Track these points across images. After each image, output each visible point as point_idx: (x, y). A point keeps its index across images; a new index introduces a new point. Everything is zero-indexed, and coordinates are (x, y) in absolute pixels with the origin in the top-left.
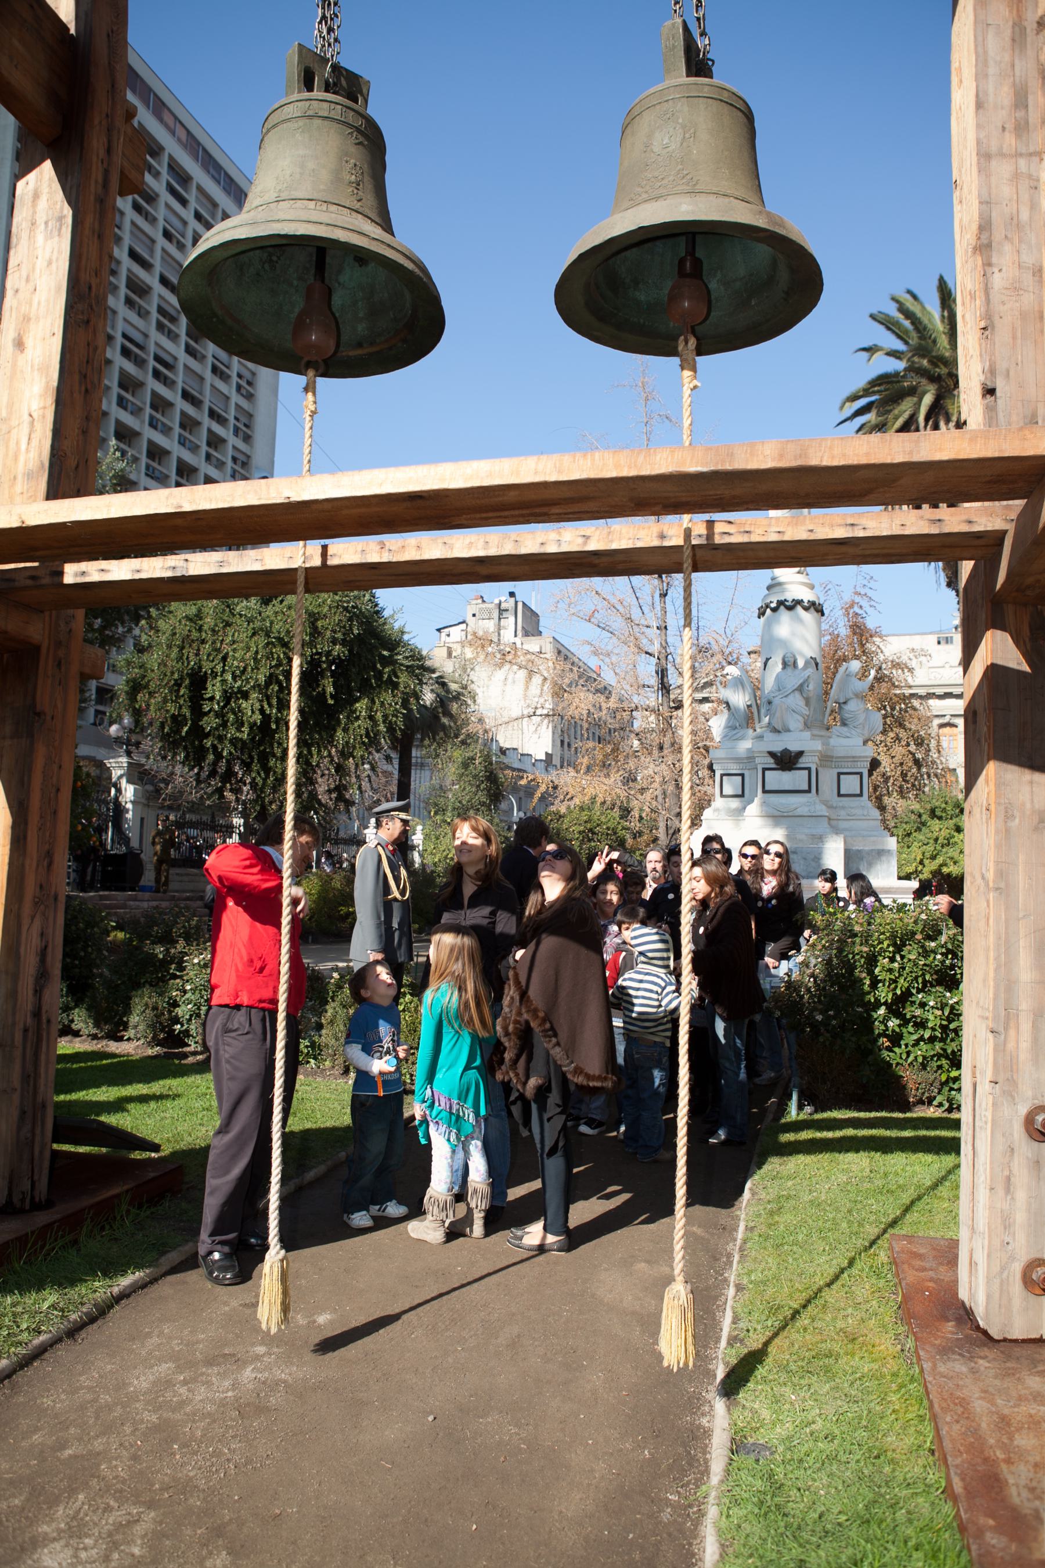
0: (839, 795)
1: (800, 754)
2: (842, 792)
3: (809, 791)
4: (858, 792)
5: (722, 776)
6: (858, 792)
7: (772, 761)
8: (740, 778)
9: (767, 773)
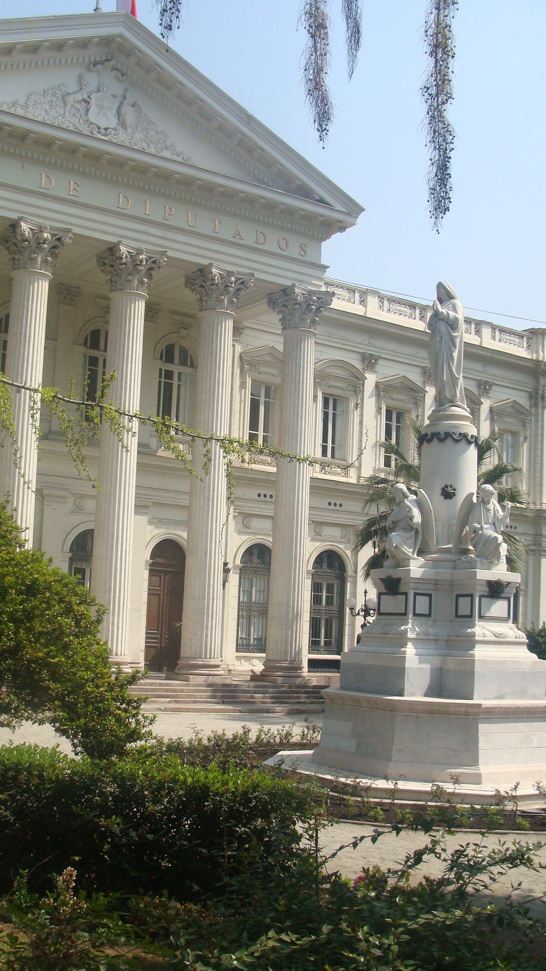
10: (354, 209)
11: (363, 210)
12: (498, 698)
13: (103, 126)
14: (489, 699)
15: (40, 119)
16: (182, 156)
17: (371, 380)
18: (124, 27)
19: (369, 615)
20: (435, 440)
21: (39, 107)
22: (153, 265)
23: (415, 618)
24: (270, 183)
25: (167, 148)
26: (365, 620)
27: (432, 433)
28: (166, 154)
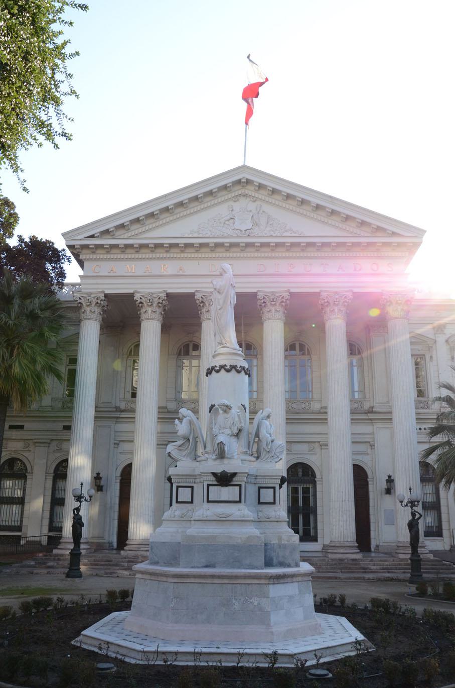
0: (259, 503)
1: (234, 474)
2: (261, 501)
3: (240, 501)
4: (272, 501)
5: (178, 487)
6: (272, 501)
7: (214, 479)
8: (190, 489)
9: (211, 488)
10: (419, 233)
11: (425, 232)
12: (206, 566)
13: (243, 229)
14: (197, 567)
15: (207, 235)
19: (415, 505)
20: (223, 371)
23: (178, 505)
25: (286, 231)
26: (412, 509)
27: (220, 366)
28: (285, 234)
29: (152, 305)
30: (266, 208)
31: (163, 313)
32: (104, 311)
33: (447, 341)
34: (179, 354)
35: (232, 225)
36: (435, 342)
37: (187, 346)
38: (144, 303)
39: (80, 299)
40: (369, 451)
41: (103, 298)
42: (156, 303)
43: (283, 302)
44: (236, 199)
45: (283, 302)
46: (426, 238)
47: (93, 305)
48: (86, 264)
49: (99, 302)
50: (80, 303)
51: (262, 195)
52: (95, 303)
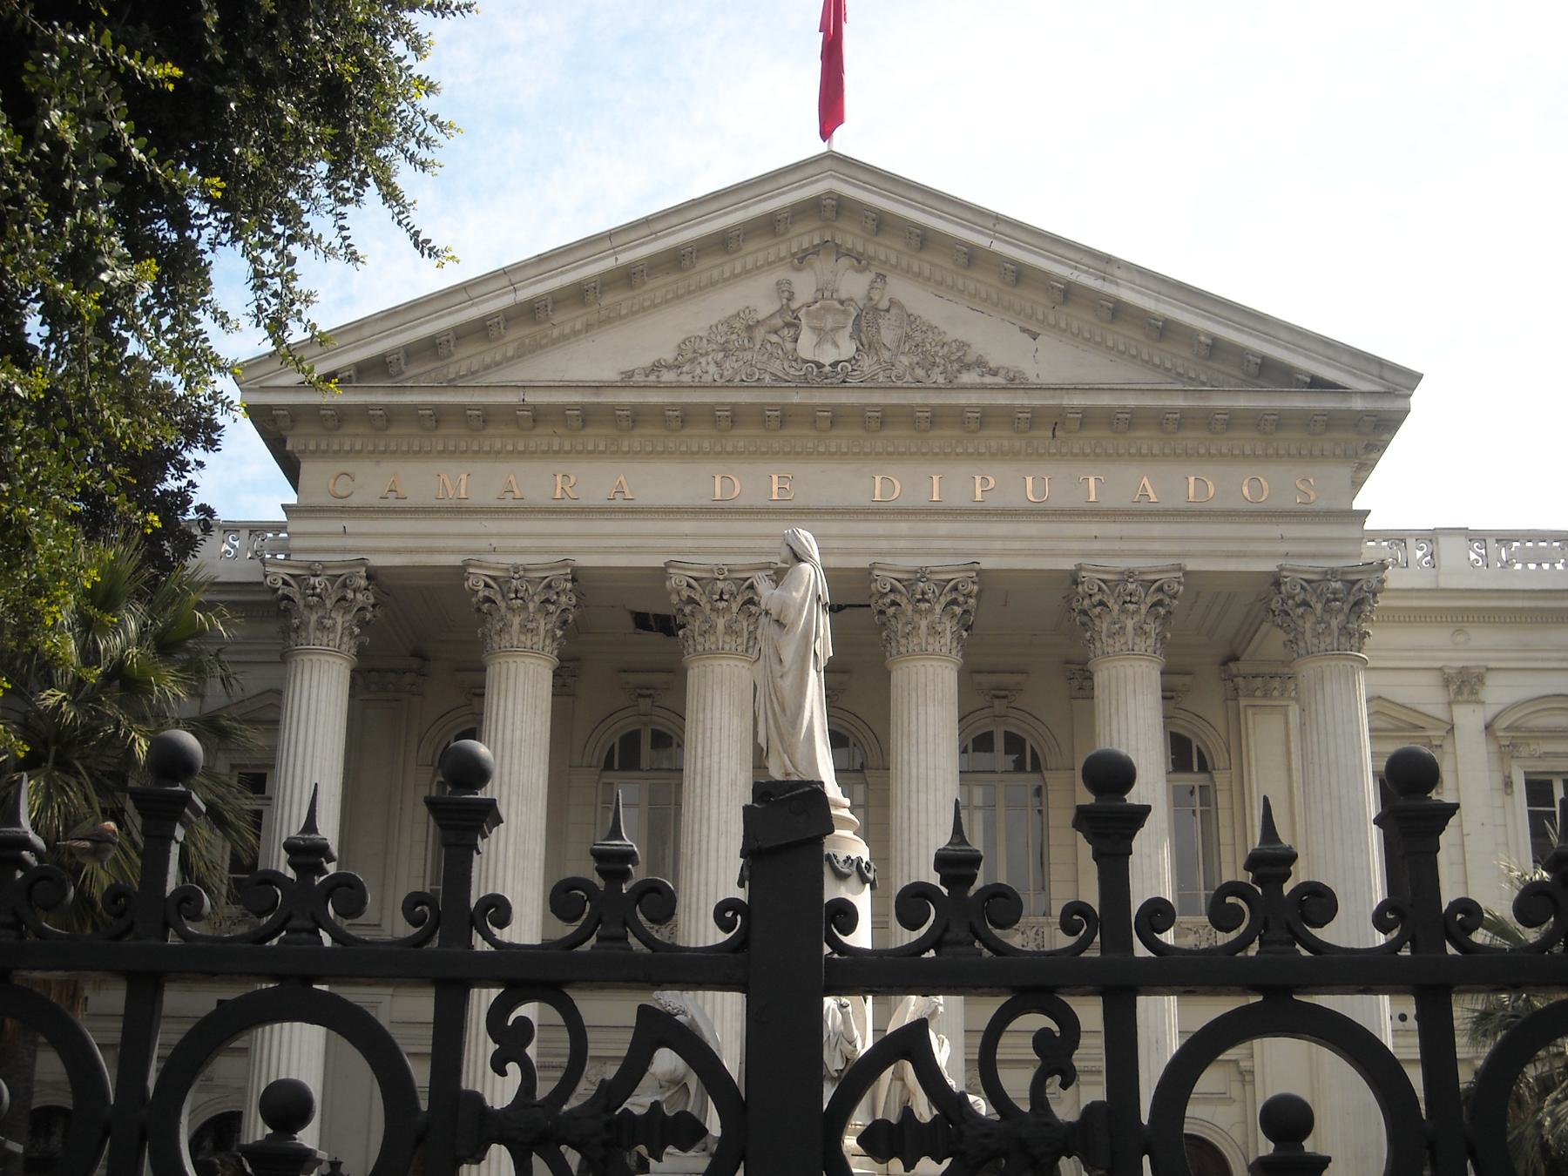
11: (1418, 377)
16: (1002, 372)
17: (1469, 720)
18: (834, 177)
21: (703, 361)
22: (1160, 596)
24: (1203, 378)
25: (968, 367)
29: (525, 607)
30: (901, 290)
31: (559, 633)
32: (363, 624)
33: (1488, 727)
34: (608, 766)
35: (789, 346)
36: (1452, 730)
37: (630, 744)
38: (498, 598)
39: (285, 583)
40: (1235, 1090)
41: (363, 583)
42: (536, 599)
43: (954, 602)
44: (801, 260)
45: (954, 602)
46: (1418, 399)
47: (329, 604)
48: (307, 469)
49: (350, 595)
50: (286, 597)
51: (887, 249)
52: (334, 599)
